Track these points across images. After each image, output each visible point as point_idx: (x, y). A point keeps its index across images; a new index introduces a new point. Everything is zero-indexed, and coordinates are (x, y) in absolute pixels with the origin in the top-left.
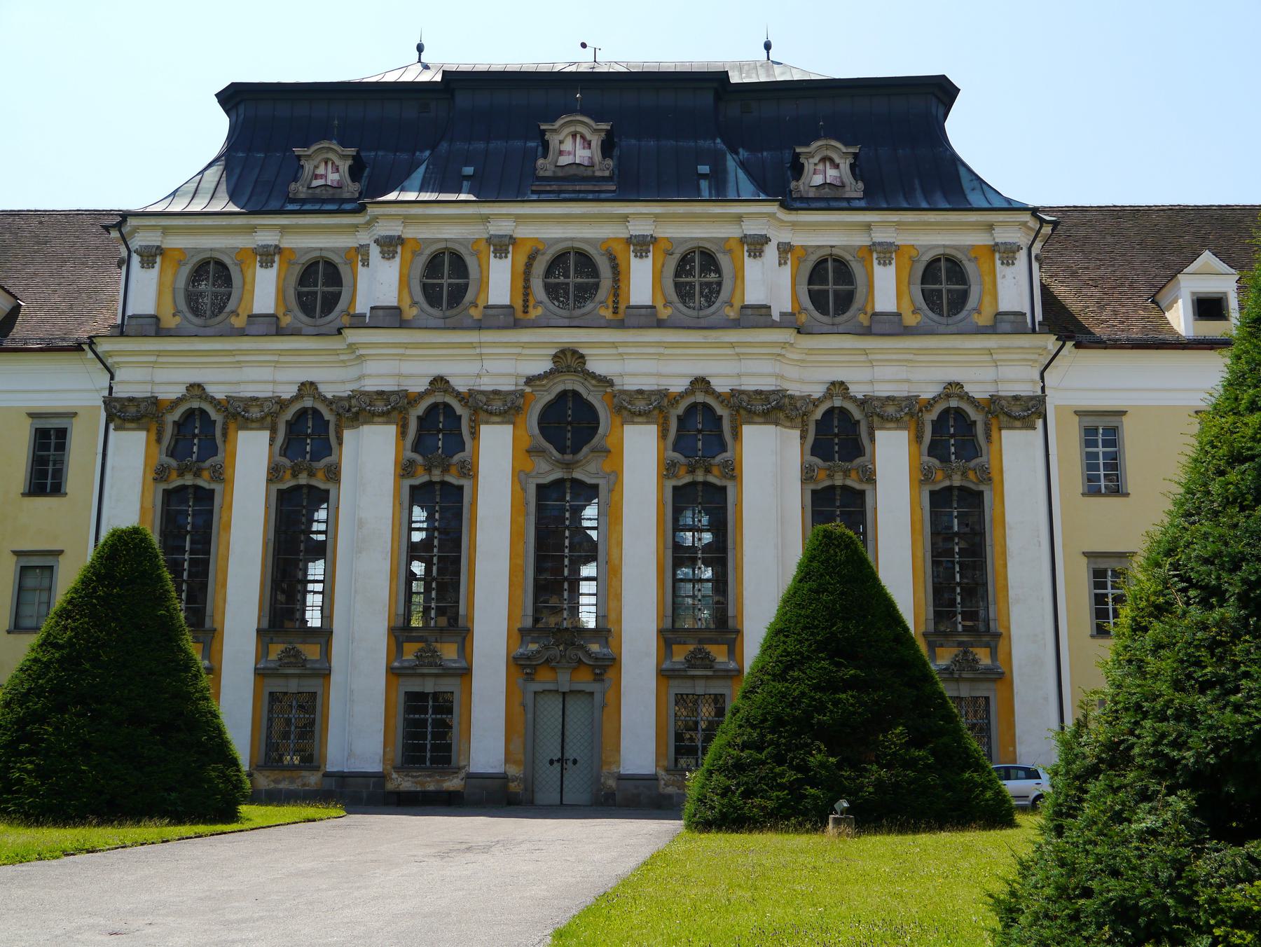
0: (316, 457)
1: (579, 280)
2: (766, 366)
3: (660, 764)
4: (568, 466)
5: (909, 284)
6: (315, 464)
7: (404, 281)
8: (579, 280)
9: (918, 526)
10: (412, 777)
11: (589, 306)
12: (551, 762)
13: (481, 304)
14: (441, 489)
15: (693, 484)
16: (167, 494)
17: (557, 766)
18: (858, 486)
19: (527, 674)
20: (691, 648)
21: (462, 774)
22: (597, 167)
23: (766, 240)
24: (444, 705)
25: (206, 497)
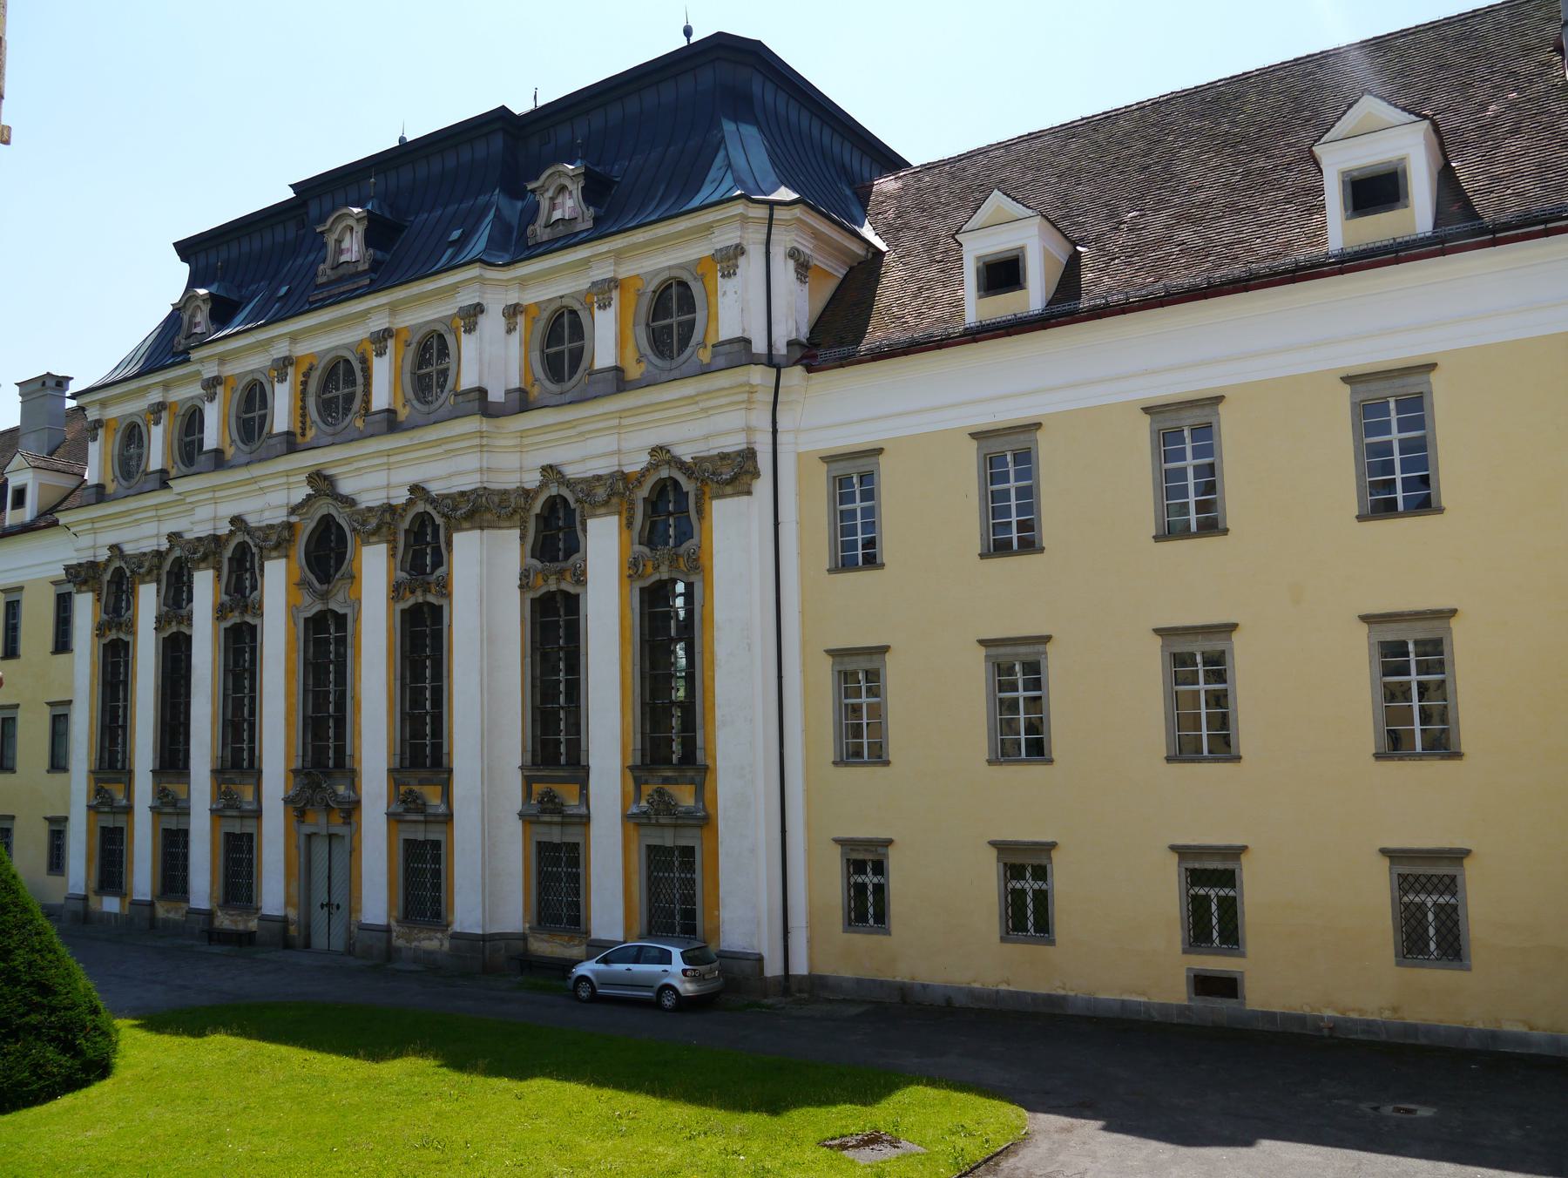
2: (471, 461)
4: (324, 596)
5: (634, 326)
9: (628, 634)
17: (326, 909)
18: (572, 590)
23: (478, 309)
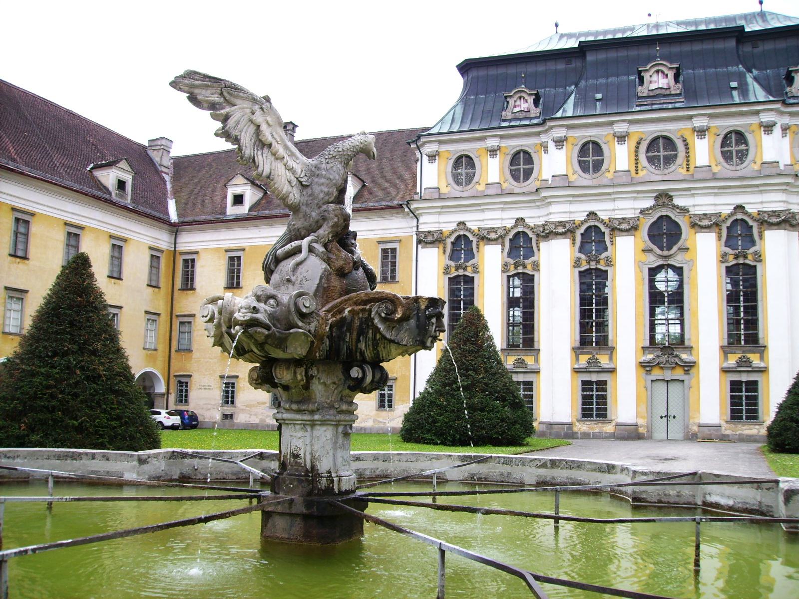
0: (526, 257)
1: (666, 153)
3: (722, 418)
6: (526, 261)
7: (569, 161)
8: (666, 153)
10: (587, 424)
11: (673, 167)
12: (661, 417)
13: (612, 170)
14: (595, 273)
15: (737, 265)
16: (451, 280)
17: (665, 419)
19: (647, 371)
20: (739, 356)
21: (614, 423)
22: (672, 89)
23: (775, 124)
24: (602, 386)
25: (470, 280)
